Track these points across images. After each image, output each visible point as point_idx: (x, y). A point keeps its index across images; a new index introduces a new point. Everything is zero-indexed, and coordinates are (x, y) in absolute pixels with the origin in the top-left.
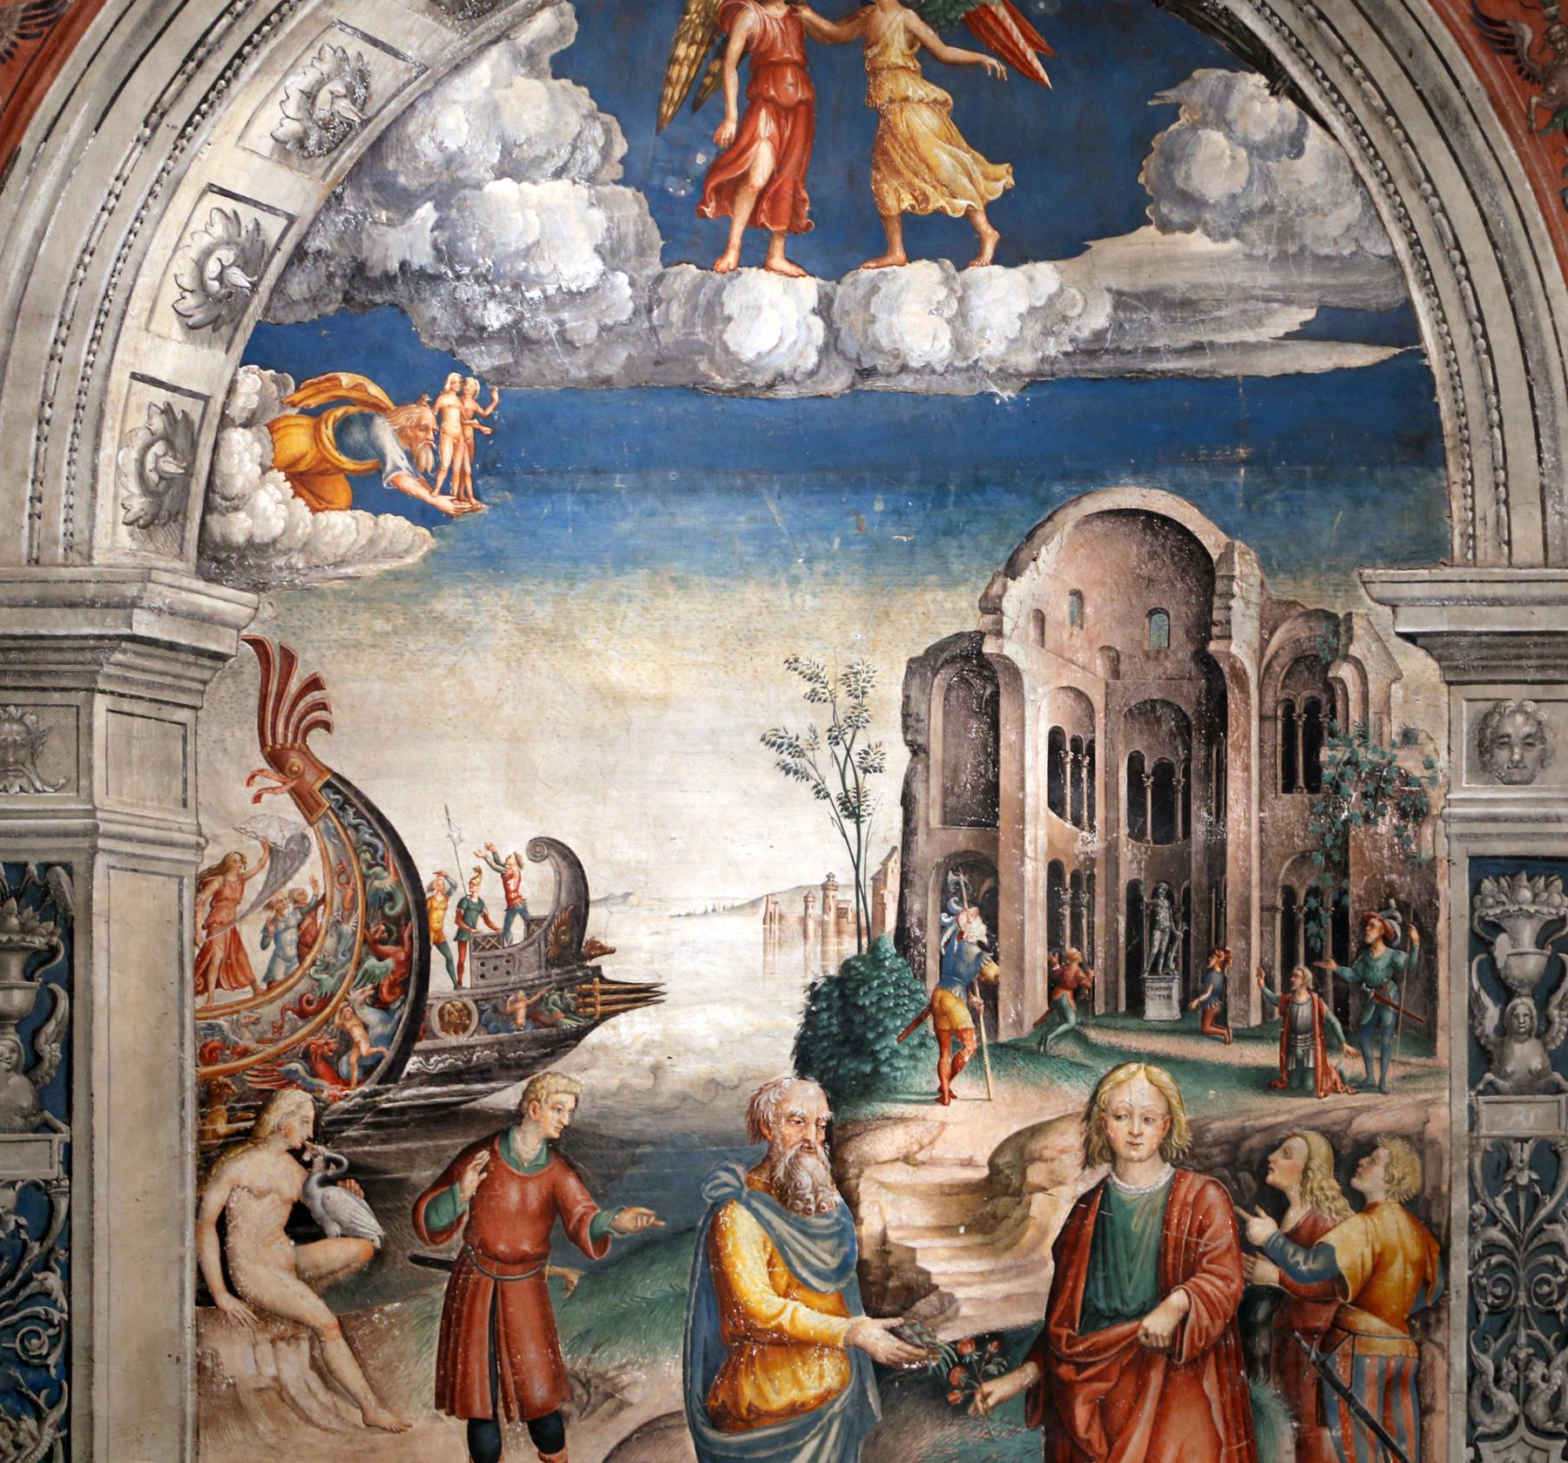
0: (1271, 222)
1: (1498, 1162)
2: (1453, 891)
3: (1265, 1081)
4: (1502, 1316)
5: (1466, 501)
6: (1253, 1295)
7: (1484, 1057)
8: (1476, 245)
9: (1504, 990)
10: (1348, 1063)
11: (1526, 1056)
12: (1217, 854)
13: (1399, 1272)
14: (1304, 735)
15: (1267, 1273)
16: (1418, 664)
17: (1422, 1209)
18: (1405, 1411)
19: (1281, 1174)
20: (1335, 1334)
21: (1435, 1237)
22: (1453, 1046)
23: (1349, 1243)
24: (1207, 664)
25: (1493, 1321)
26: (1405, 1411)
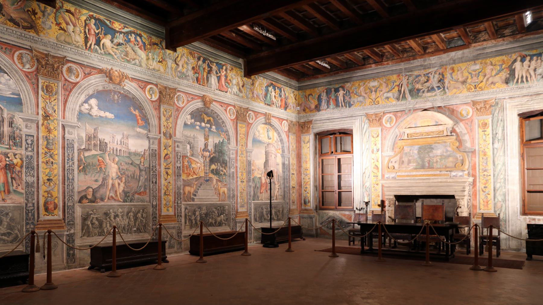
0: (9, 86)
1: (27, 157)
2: (24, 137)
3: (8, 149)
4: (28, 168)
5: (25, 108)
6: (6, 164)
7: (26, 149)
8: (25, 90)
9: (28, 144)
10: (15, 148)
11: (30, 149)
12: (3, 131)
13: (19, 164)
14: (11, 124)
15: (8, 163)
16: (21, 120)
17: (21, 159)
18: (20, 174)
19: (9, 155)
20: (14, 168)
21: (22, 161)
22: (24, 147)
23: (15, 161)
24: (2, 117)
25: (27, 168)
26: (20, 174)
